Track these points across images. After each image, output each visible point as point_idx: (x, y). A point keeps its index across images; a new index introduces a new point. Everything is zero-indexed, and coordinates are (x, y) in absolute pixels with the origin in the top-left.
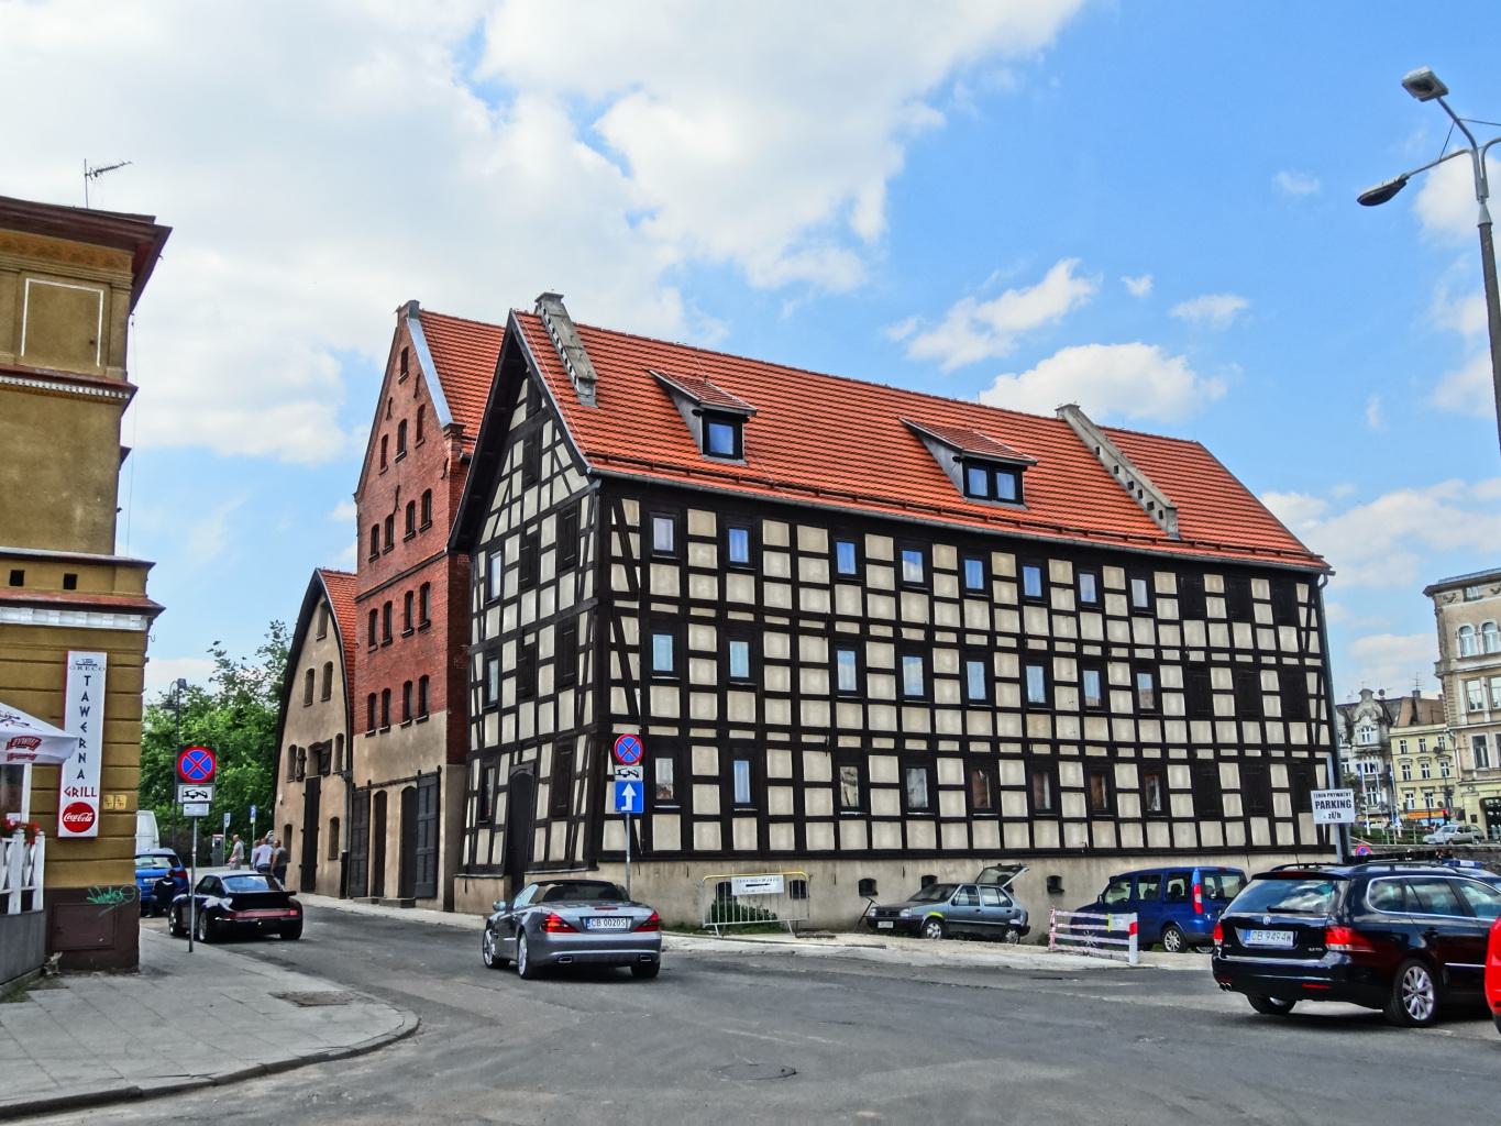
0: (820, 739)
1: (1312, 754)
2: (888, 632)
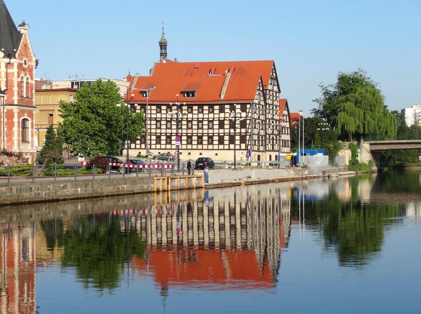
0: (154, 134)
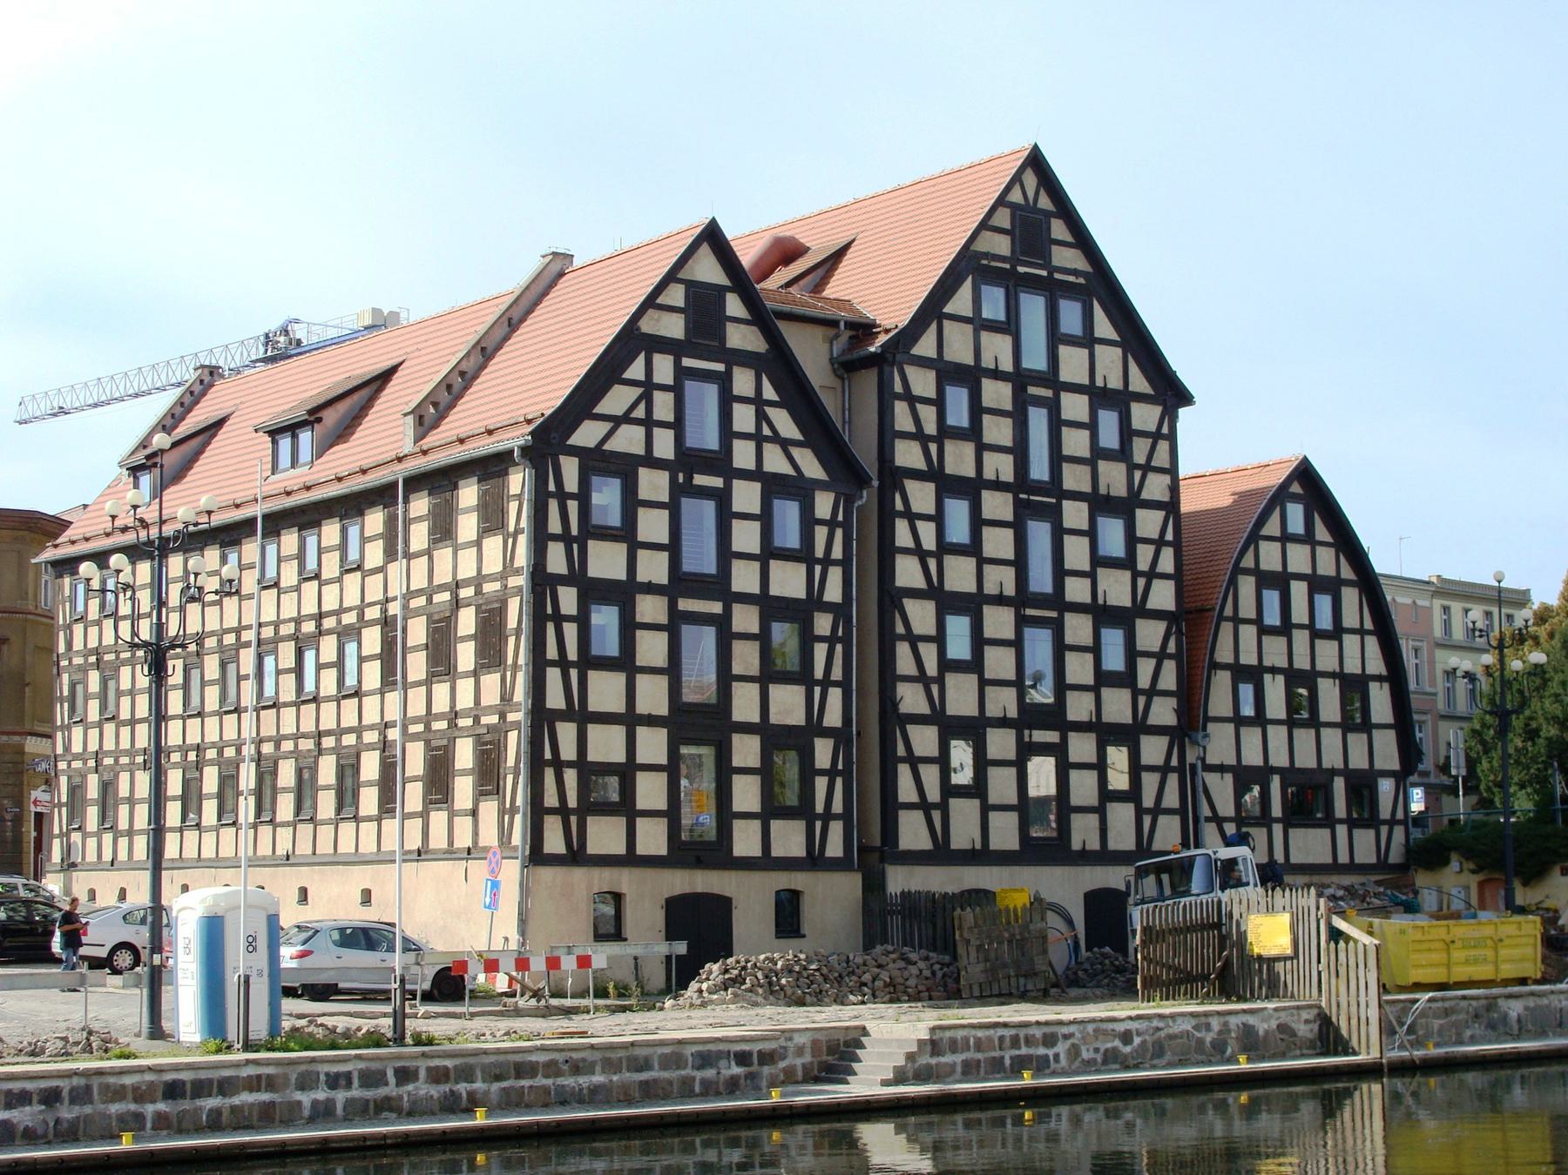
1: (503, 716)
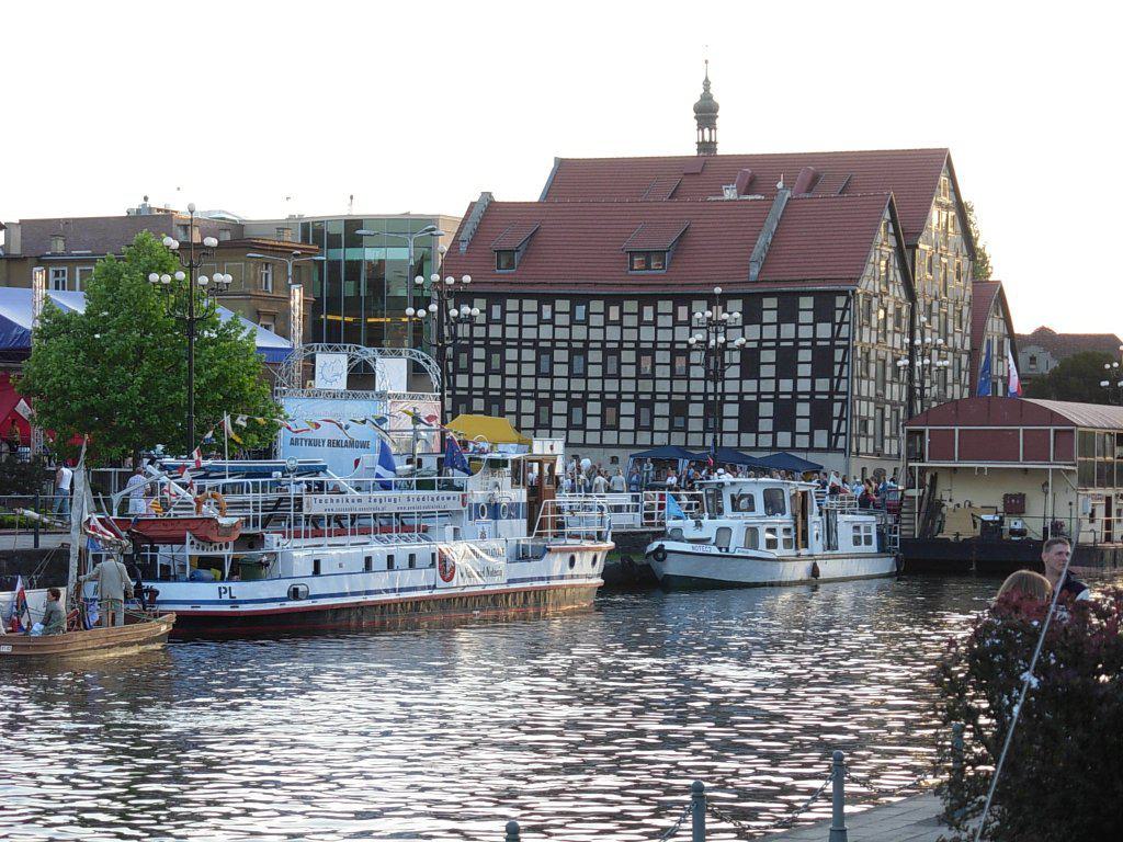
0: (529, 394)
2: (565, 345)
